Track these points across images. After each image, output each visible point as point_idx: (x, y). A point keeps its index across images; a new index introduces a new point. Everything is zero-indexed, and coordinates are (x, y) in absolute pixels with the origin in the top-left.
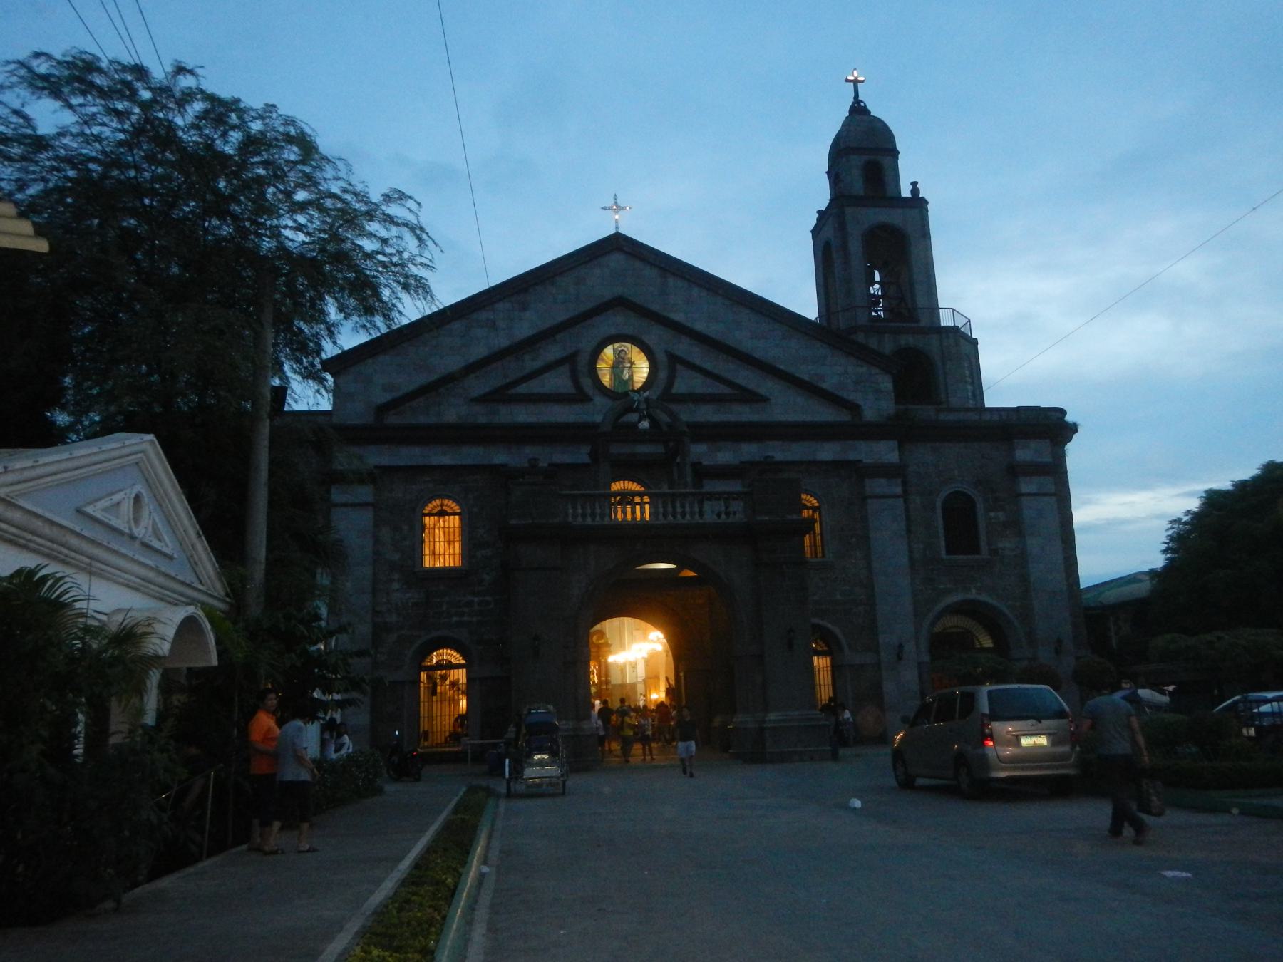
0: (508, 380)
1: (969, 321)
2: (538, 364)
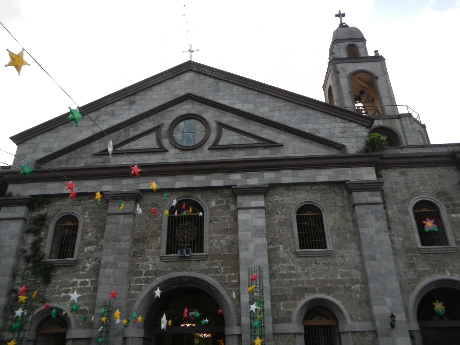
1: (419, 116)
2: (139, 132)
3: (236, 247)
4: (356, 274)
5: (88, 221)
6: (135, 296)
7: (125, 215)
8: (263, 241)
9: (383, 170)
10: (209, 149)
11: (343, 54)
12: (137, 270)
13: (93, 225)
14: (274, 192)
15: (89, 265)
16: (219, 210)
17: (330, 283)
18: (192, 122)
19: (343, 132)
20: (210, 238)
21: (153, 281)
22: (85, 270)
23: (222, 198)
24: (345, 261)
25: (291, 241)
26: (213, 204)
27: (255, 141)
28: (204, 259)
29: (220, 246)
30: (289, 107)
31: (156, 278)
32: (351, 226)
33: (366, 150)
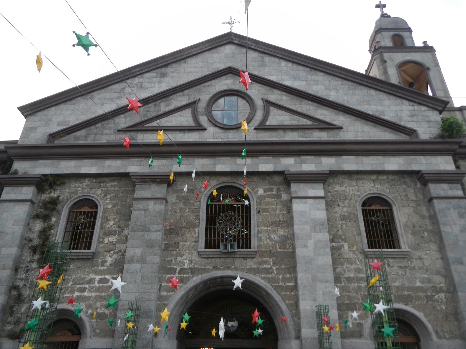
0: (146, 118)
2: (171, 108)
3: (291, 243)
4: (440, 281)
5: (110, 206)
6: (167, 298)
7: (155, 201)
8: (325, 236)
9: (460, 160)
10: (254, 129)
11: (388, 43)
12: (169, 267)
13: (115, 212)
14: (334, 181)
15: (109, 260)
16: (268, 199)
17: (408, 291)
18: (233, 99)
19: (411, 116)
20: (258, 232)
21: (189, 280)
22: (105, 264)
23: (271, 185)
24: (424, 265)
25: (358, 238)
26: (261, 192)
27: (308, 122)
28: (252, 256)
29: (270, 241)
30: (347, 86)
31: (193, 277)
32: (428, 224)
33: (441, 136)
